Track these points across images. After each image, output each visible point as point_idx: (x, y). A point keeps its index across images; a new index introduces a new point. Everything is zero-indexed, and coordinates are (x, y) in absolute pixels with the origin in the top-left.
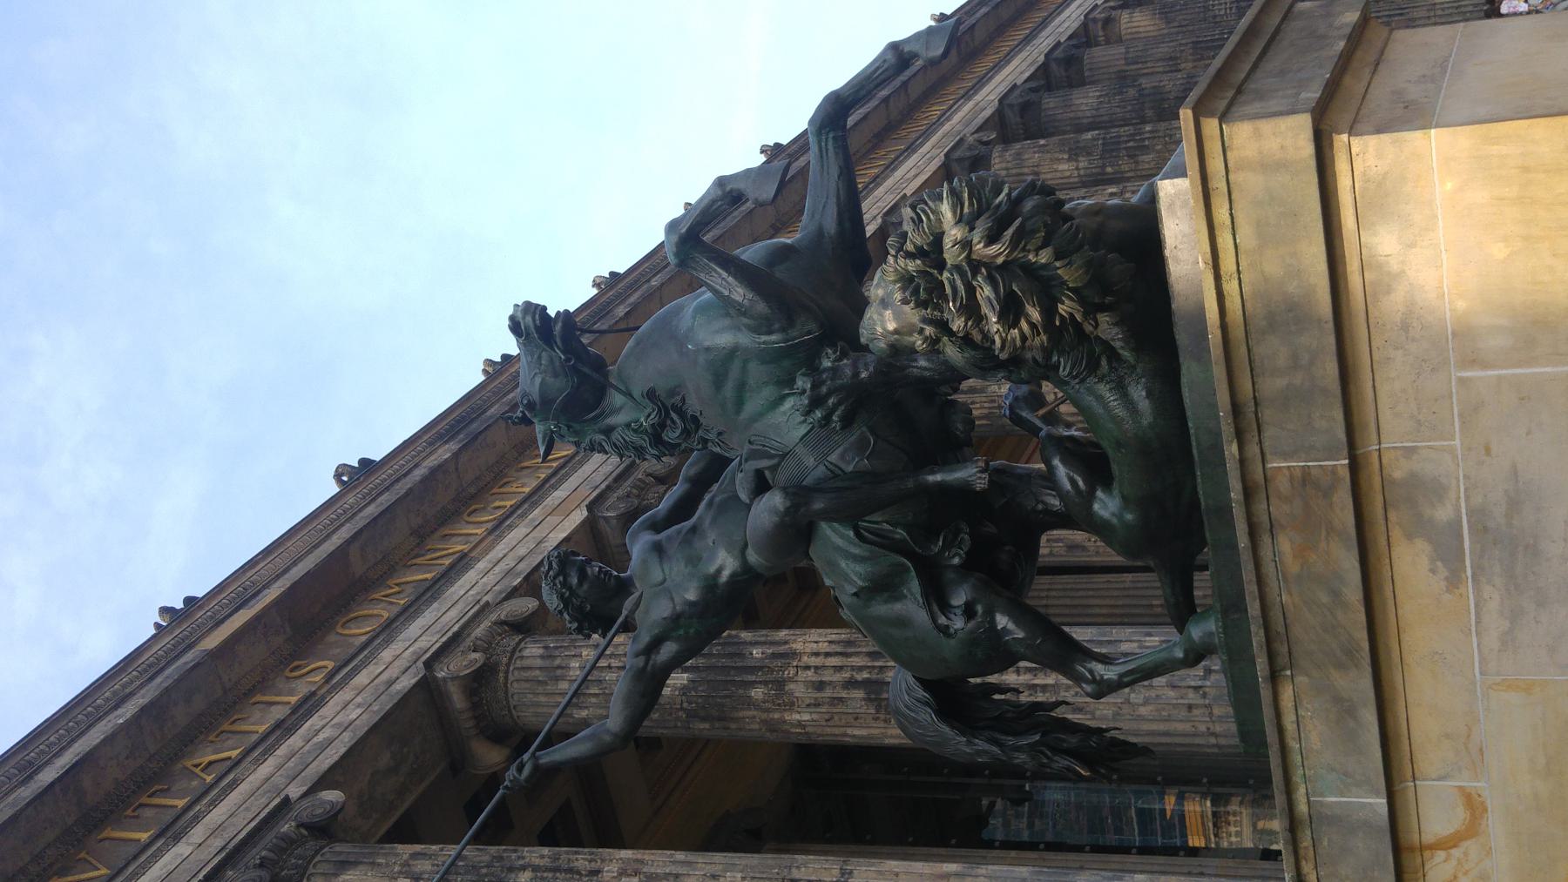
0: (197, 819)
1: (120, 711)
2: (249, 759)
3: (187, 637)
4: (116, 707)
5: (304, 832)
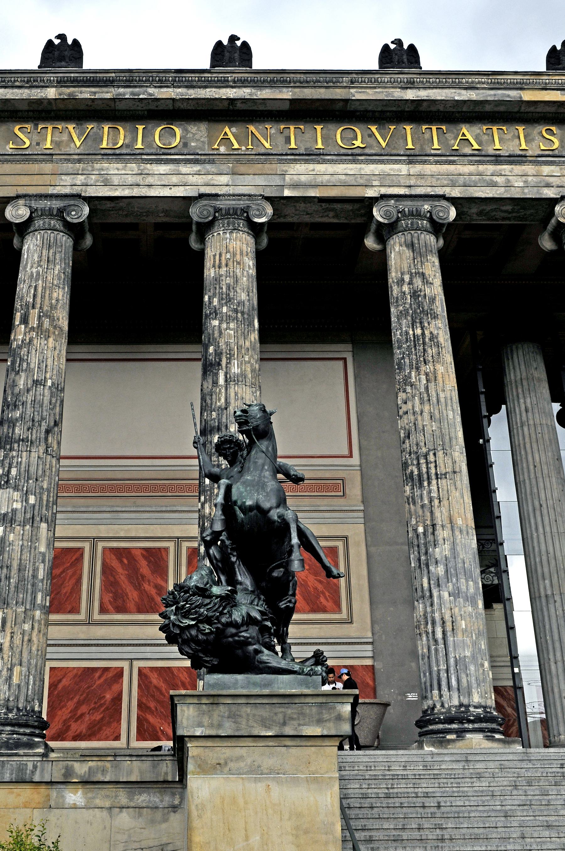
0: (424, 162)
1: (463, 92)
2: (470, 158)
3: (526, 84)
4: (466, 89)
5: (428, 215)
